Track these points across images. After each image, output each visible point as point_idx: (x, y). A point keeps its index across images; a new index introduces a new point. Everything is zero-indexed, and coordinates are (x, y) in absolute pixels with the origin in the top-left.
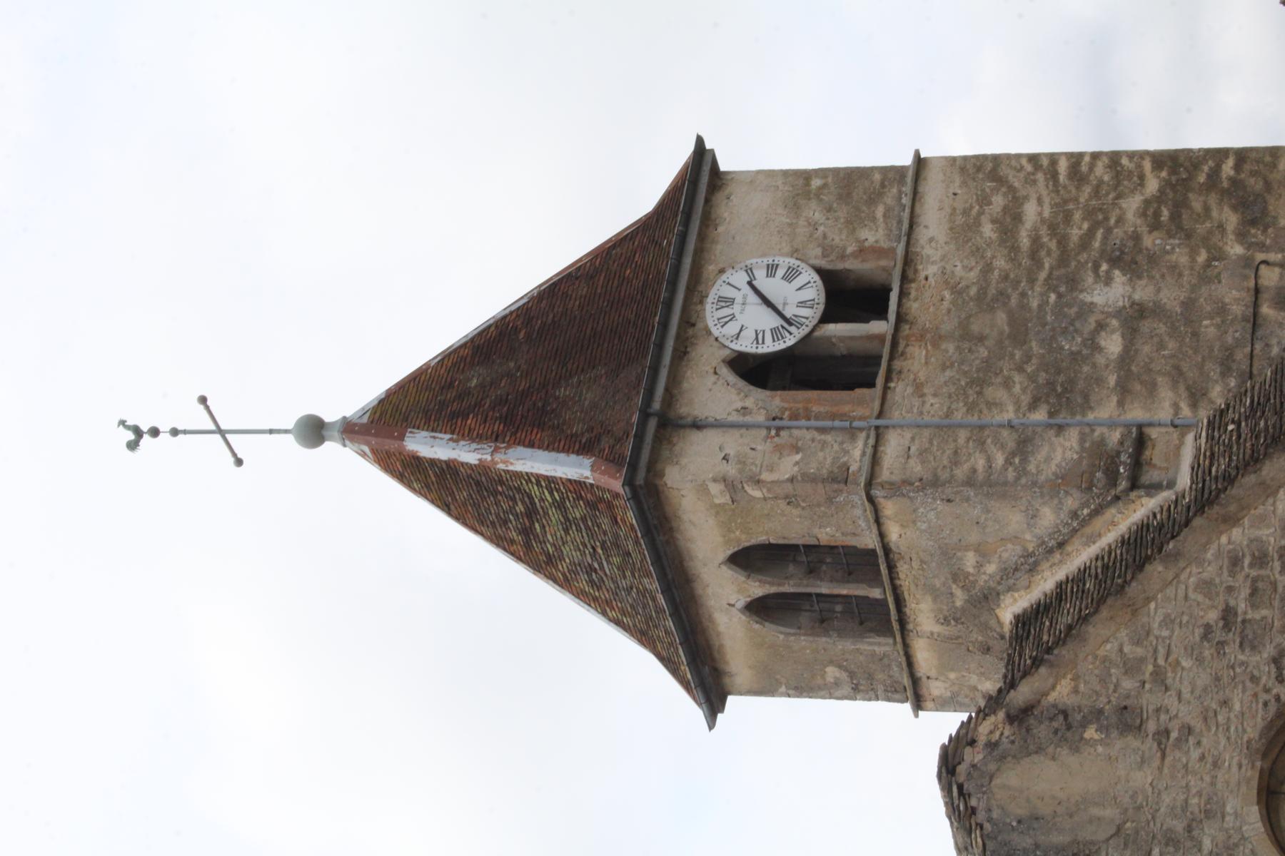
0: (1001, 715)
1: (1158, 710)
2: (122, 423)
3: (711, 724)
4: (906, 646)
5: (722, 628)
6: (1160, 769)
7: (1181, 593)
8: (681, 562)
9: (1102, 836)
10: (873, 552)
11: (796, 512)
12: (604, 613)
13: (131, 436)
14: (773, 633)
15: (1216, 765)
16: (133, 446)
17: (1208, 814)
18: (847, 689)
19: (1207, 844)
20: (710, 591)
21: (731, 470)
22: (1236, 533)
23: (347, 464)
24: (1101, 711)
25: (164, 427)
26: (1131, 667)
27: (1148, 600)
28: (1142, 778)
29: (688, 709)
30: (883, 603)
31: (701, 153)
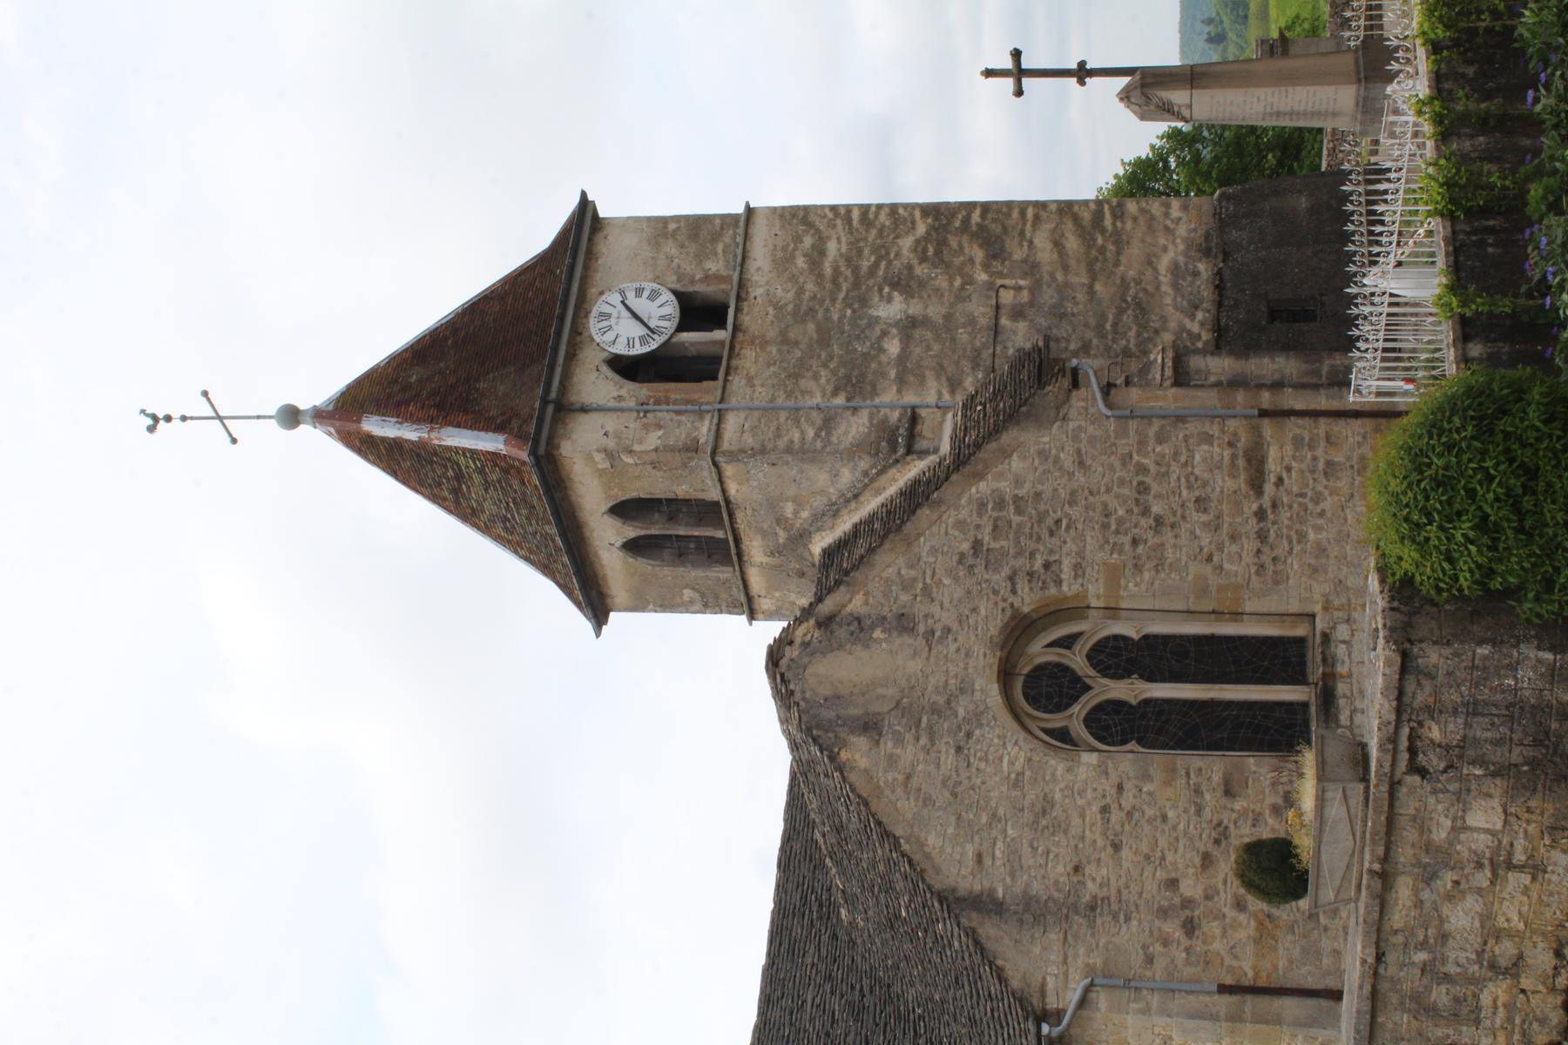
0: (812, 622)
1: (926, 616)
2: (143, 412)
3: (598, 634)
4: (742, 573)
6: (928, 659)
7: (943, 531)
9: (886, 708)
10: (717, 503)
11: (659, 474)
12: (516, 552)
13: (150, 422)
14: (643, 565)
15: (967, 655)
16: (151, 429)
17: (962, 691)
18: (699, 606)
19: (961, 712)
21: (610, 443)
22: (982, 485)
23: (319, 443)
24: (884, 618)
25: (176, 415)
26: (907, 585)
27: (919, 535)
28: (914, 666)
29: (583, 624)
30: (726, 541)
31: (585, 205)
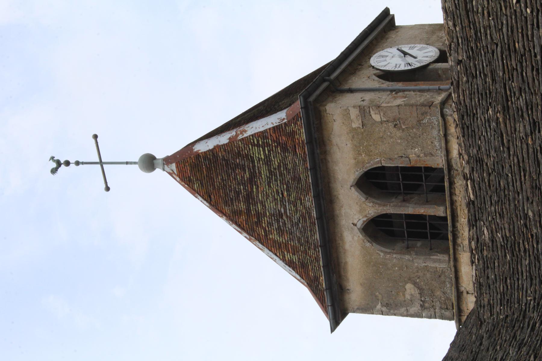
3: (332, 331)
4: (456, 260)
5: (347, 246)
8: (329, 183)
10: (441, 170)
11: (399, 134)
12: (283, 260)
13: (54, 165)
14: (379, 252)
16: (54, 171)
18: (415, 308)
20: (343, 211)
21: (364, 103)
25: (72, 161)
29: (323, 320)
30: (445, 219)
